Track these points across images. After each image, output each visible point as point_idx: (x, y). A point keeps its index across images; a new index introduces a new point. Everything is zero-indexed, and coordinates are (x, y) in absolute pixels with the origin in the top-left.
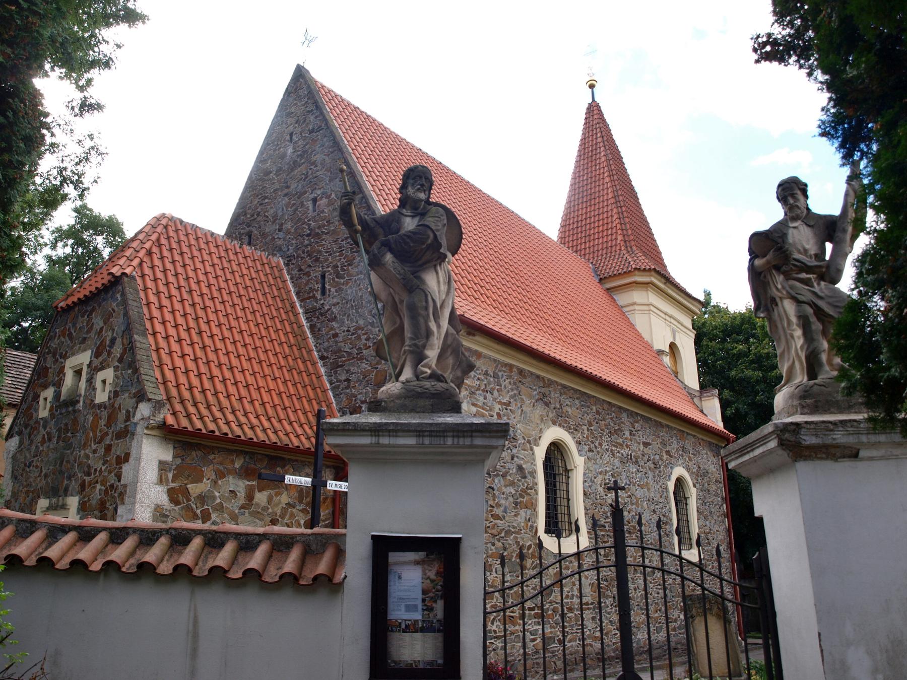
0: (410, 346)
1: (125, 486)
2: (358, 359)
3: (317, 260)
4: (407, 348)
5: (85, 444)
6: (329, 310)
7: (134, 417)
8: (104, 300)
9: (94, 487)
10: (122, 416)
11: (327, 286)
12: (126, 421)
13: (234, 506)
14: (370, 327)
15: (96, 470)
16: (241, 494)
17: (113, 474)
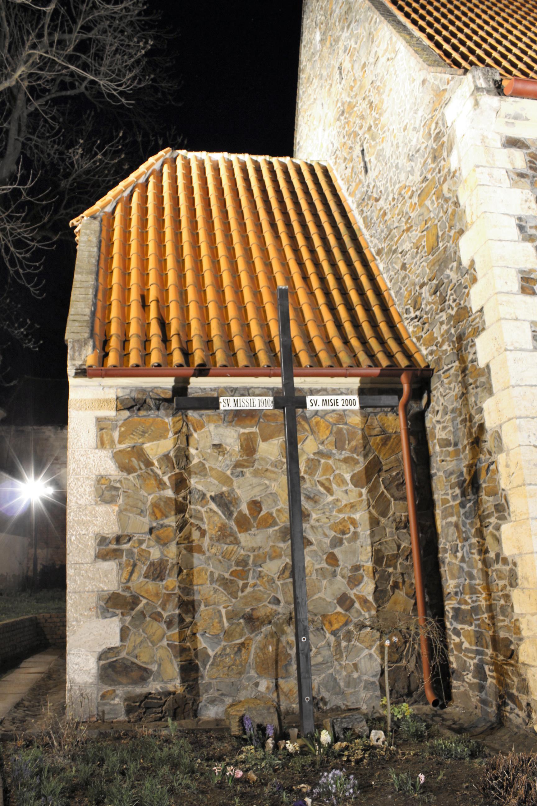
6: (374, 187)
11: (367, 159)
13: (222, 464)
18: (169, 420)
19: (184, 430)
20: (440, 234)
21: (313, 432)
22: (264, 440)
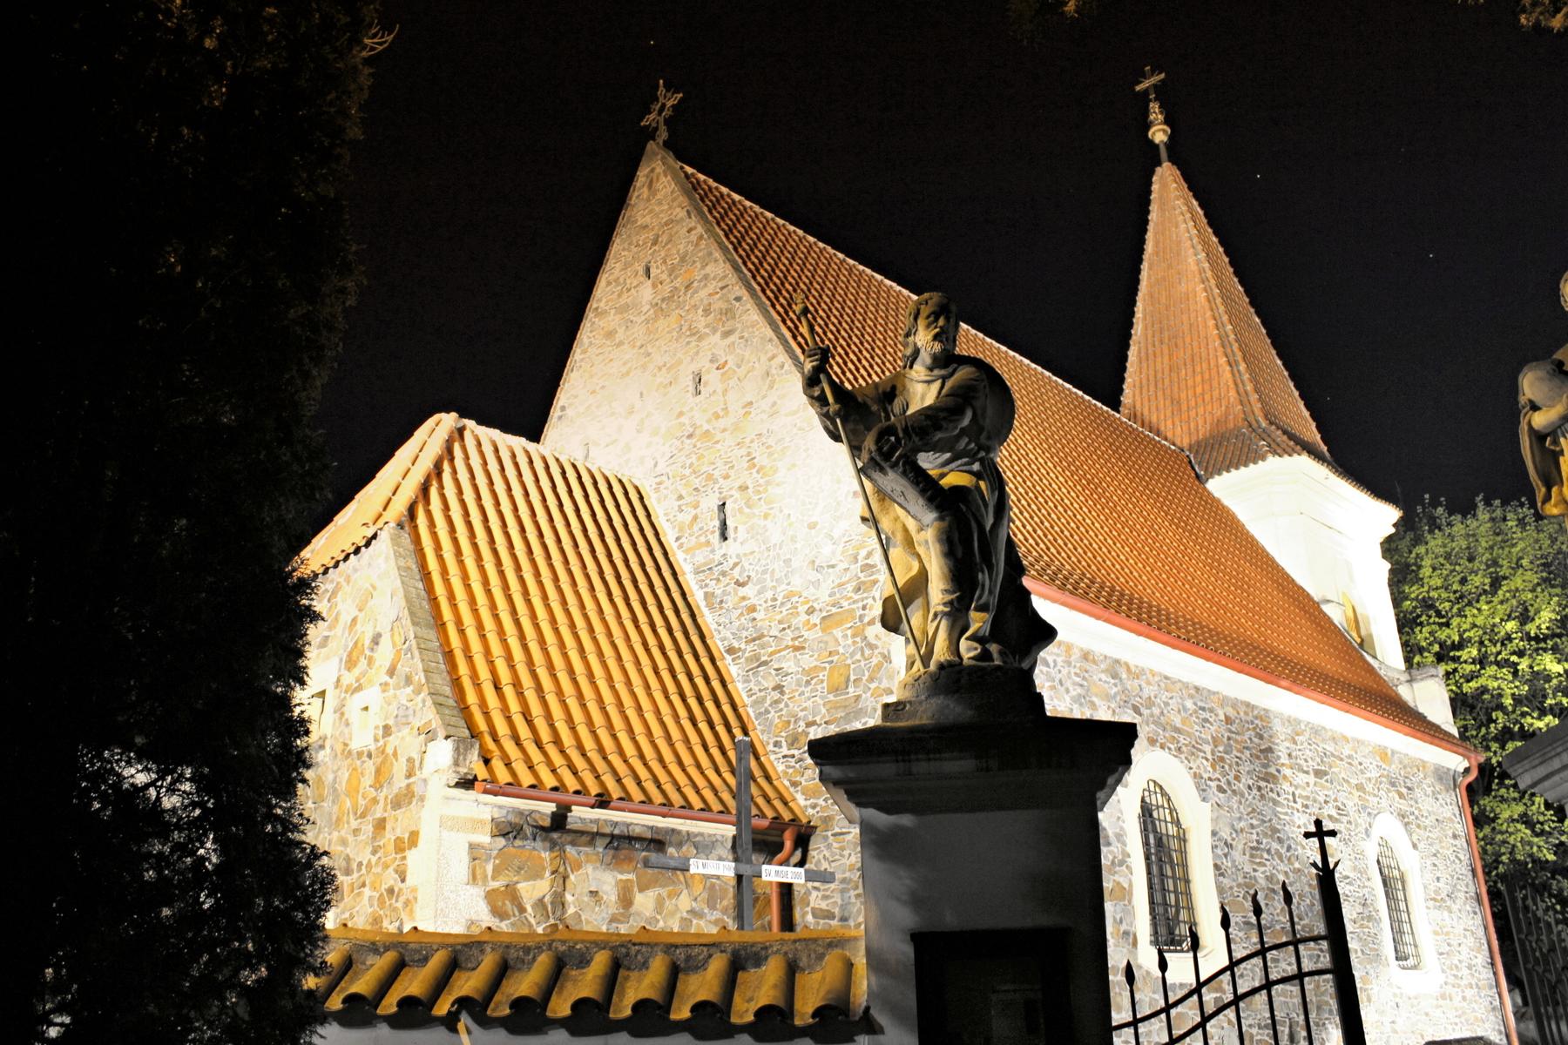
0: (945, 604)
1: (414, 890)
2: (797, 649)
3: (710, 477)
4: (941, 608)
5: (338, 820)
6: (736, 565)
7: (421, 768)
8: (356, 570)
9: (359, 894)
10: (400, 768)
12: (409, 776)
14: (812, 590)
15: (360, 864)
16: (610, 894)
17: (391, 870)
18: (546, 855)
19: (561, 869)
20: (852, 678)
21: (687, 886)
22: (641, 891)
